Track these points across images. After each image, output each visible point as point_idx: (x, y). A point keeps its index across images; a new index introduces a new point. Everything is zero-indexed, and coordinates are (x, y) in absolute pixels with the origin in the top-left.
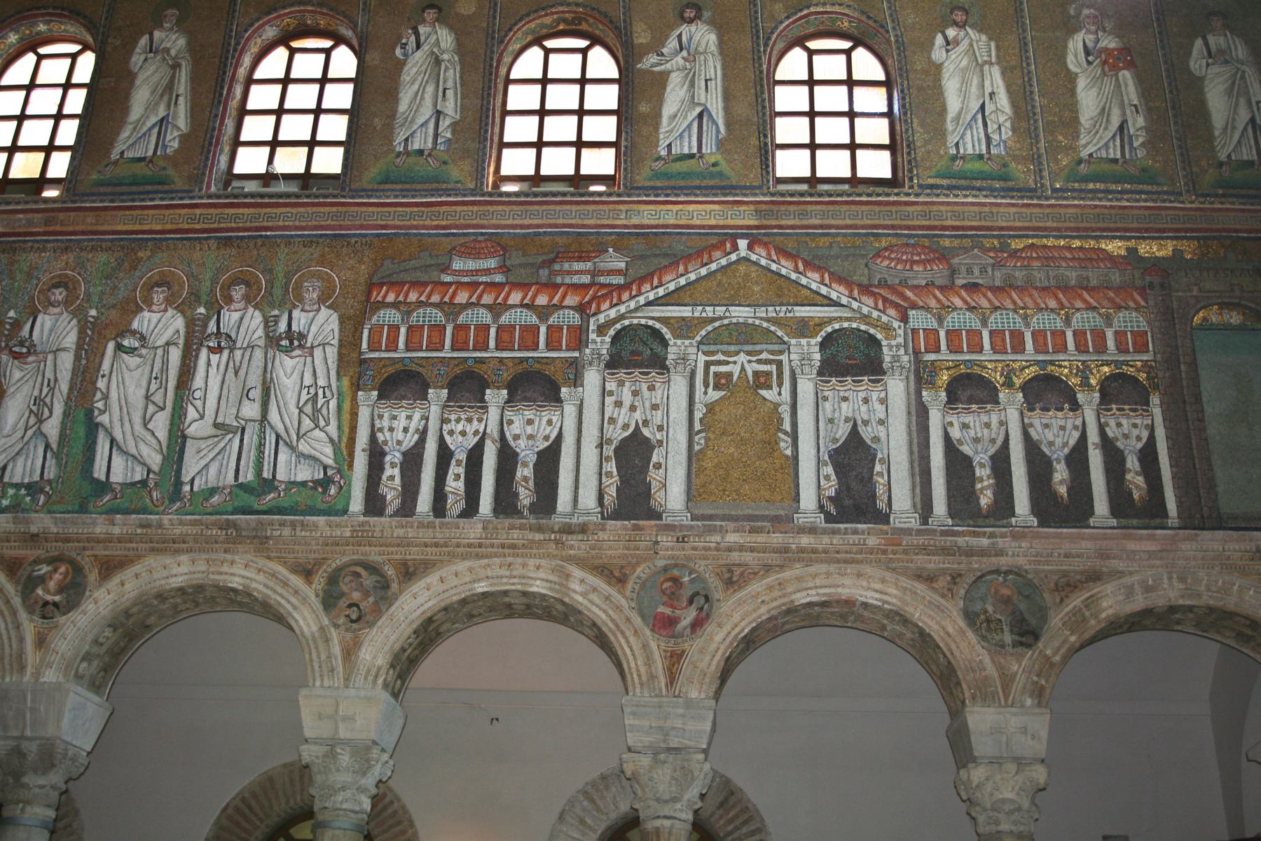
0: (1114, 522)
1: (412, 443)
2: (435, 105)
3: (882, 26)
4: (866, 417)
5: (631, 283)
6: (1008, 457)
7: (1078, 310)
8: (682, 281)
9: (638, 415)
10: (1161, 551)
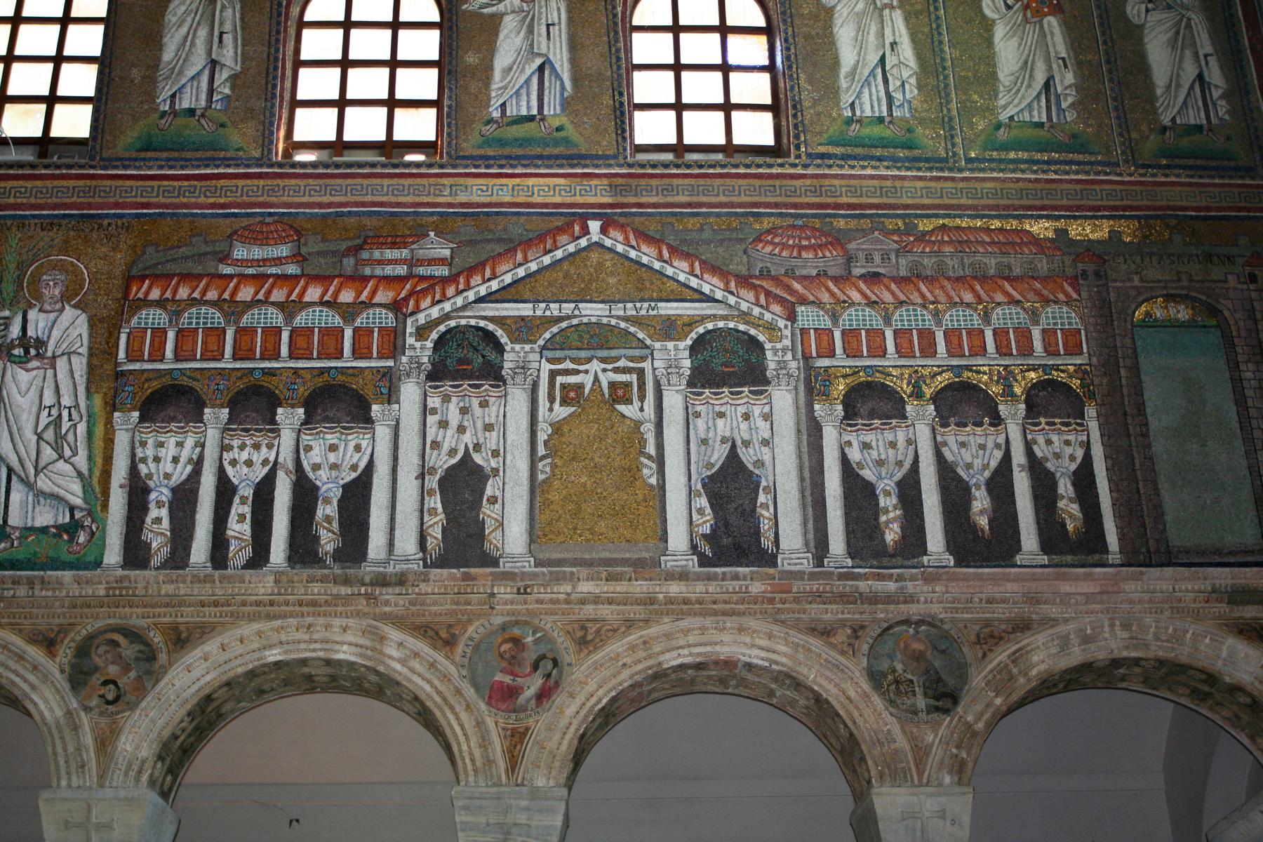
0: (1045, 559)
1: (184, 477)
2: (209, 52)
4: (746, 437)
5: (458, 275)
6: (918, 482)
8: (521, 272)
9: (468, 438)
10: (1102, 593)
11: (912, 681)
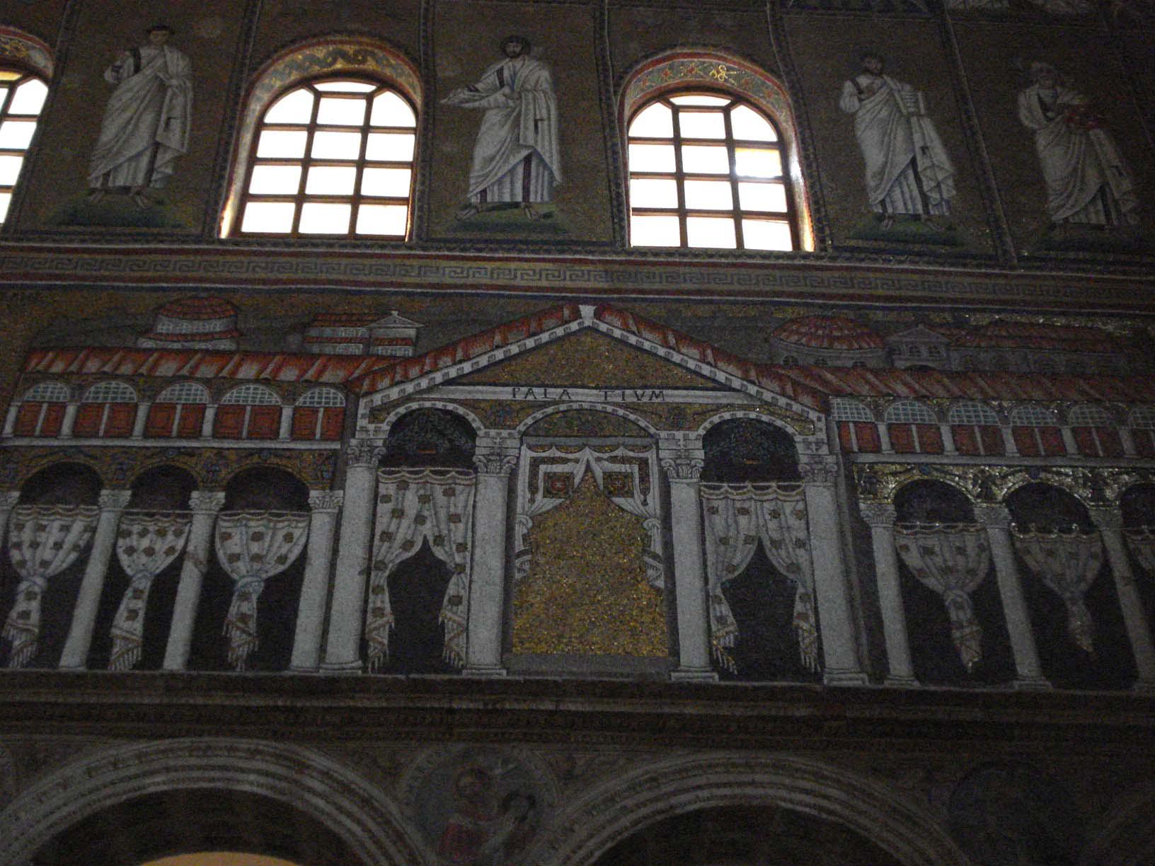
1: (65, 566)
2: (154, 133)
3: (772, 71)
4: (776, 536)
5: (426, 355)
7: (1076, 402)
8: (499, 355)
9: (428, 529)
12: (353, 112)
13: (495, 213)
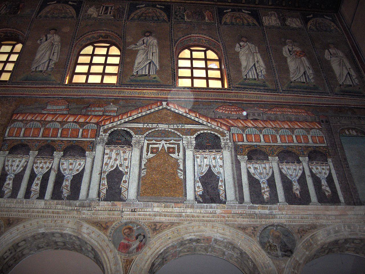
1: (20, 171)
2: (49, 57)
4: (214, 164)
5: (119, 115)
6: (274, 180)
8: (140, 115)
9: (118, 162)
10: (340, 215)
11: (276, 246)
12: (104, 51)
13: (140, 77)
